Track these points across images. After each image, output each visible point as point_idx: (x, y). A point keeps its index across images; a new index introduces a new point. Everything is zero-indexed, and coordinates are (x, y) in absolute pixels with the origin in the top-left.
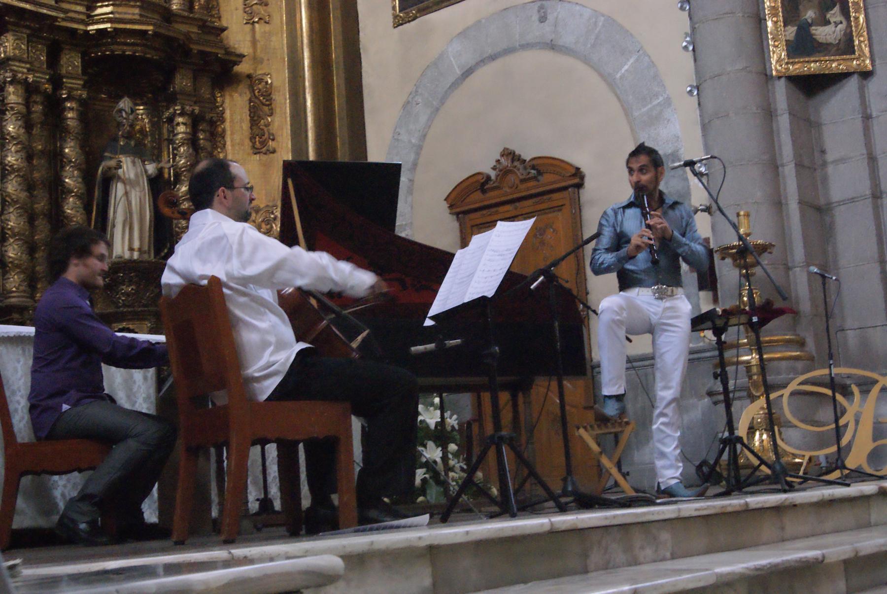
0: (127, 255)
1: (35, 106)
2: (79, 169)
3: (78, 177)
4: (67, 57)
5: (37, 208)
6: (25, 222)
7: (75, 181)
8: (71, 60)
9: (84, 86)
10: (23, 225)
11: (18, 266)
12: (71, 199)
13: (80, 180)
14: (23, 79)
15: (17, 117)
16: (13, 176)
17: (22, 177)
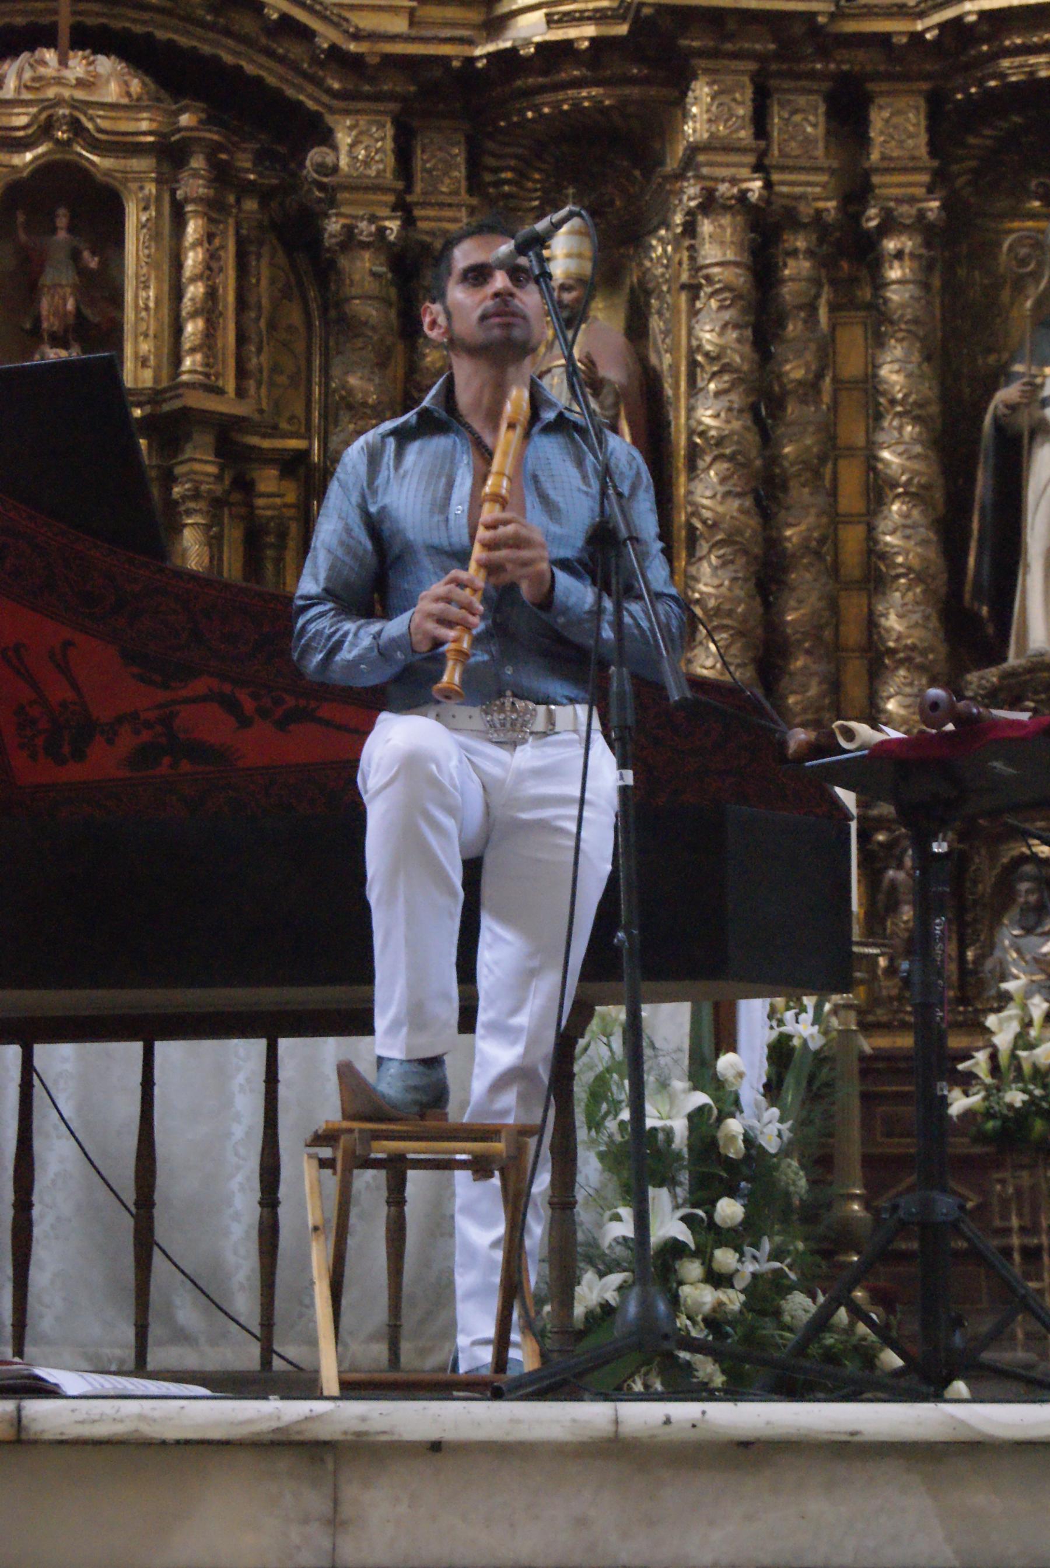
1: (791, 262)
2: (917, 420)
3: (915, 440)
4: (886, 114)
5: (789, 539)
6: (734, 580)
7: (900, 454)
8: (895, 120)
9: (930, 189)
10: (730, 589)
12: (895, 507)
13: (918, 449)
14: (732, 197)
15: (720, 301)
16: (708, 459)
17: (731, 458)
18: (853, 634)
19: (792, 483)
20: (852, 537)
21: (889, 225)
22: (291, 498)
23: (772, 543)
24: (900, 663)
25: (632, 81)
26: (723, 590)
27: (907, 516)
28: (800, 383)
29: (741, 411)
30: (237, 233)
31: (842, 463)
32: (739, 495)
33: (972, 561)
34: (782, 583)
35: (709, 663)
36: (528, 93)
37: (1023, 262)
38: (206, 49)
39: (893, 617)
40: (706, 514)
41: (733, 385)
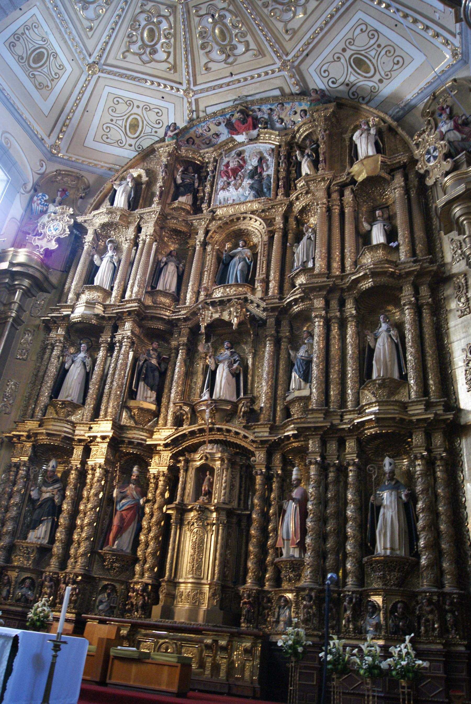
3: (353, 509)
6: (312, 539)
9: (357, 457)
21: (349, 464)
25: (302, 441)
28: (330, 498)
30: (240, 474)
36: (288, 444)
37: (371, 471)
38: (235, 441)
41: (314, 499)
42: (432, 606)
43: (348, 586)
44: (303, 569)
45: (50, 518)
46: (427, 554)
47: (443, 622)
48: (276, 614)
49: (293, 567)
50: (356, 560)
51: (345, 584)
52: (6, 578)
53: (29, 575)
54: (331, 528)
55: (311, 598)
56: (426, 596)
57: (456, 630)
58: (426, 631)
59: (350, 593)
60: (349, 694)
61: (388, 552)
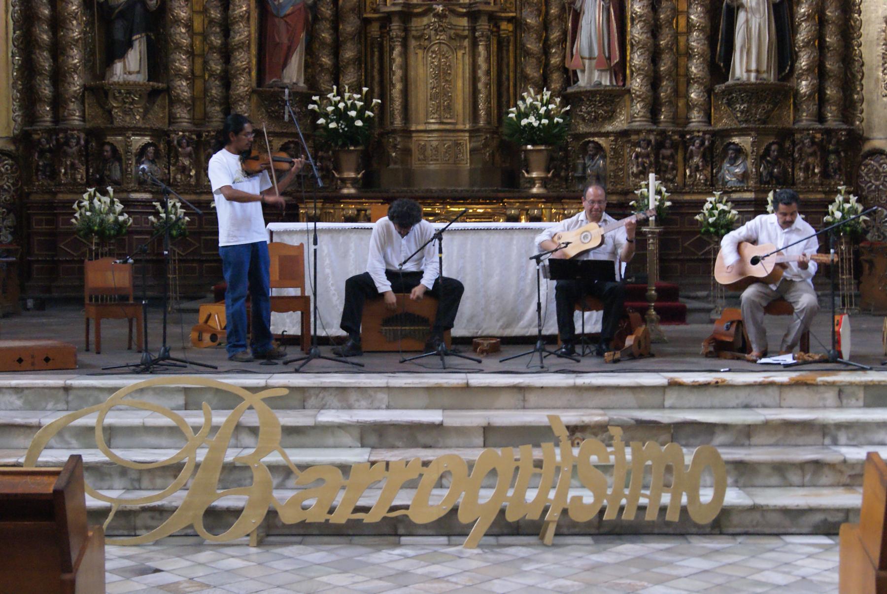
0: (745, 76)
2: (702, 6)
3: (701, 12)
6: (644, 59)
11: (639, 96)
13: (702, 15)
18: (682, 71)
19: (663, 27)
20: (682, 40)
22: (511, 29)
23: (656, 46)
24: (695, 82)
26: (641, 63)
27: (698, 36)
29: (647, 6)
31: (680, 17)
32: (646, 33)
33: (718, 48)
34: (660, 59)
35: (637, 85)
39: (693, 68)
40: (637, 39)
42: (815, 147)
43: (692, 125)
44: (619, 102)
45: (143, 34)
46: (809, 78)
47: (825, 165)
48: (580, 168)
49: (605, 101)
50: (705, 87)
51: (688, 120)
52: (107, 148)
53: (147, 139)
54: (668, 42)
55: (649, 143)
56: (809, 134)
57: (840, 175)
58: (806, 178)
59: (701, 134)
60: (698, 260)
61: (753, 75)
